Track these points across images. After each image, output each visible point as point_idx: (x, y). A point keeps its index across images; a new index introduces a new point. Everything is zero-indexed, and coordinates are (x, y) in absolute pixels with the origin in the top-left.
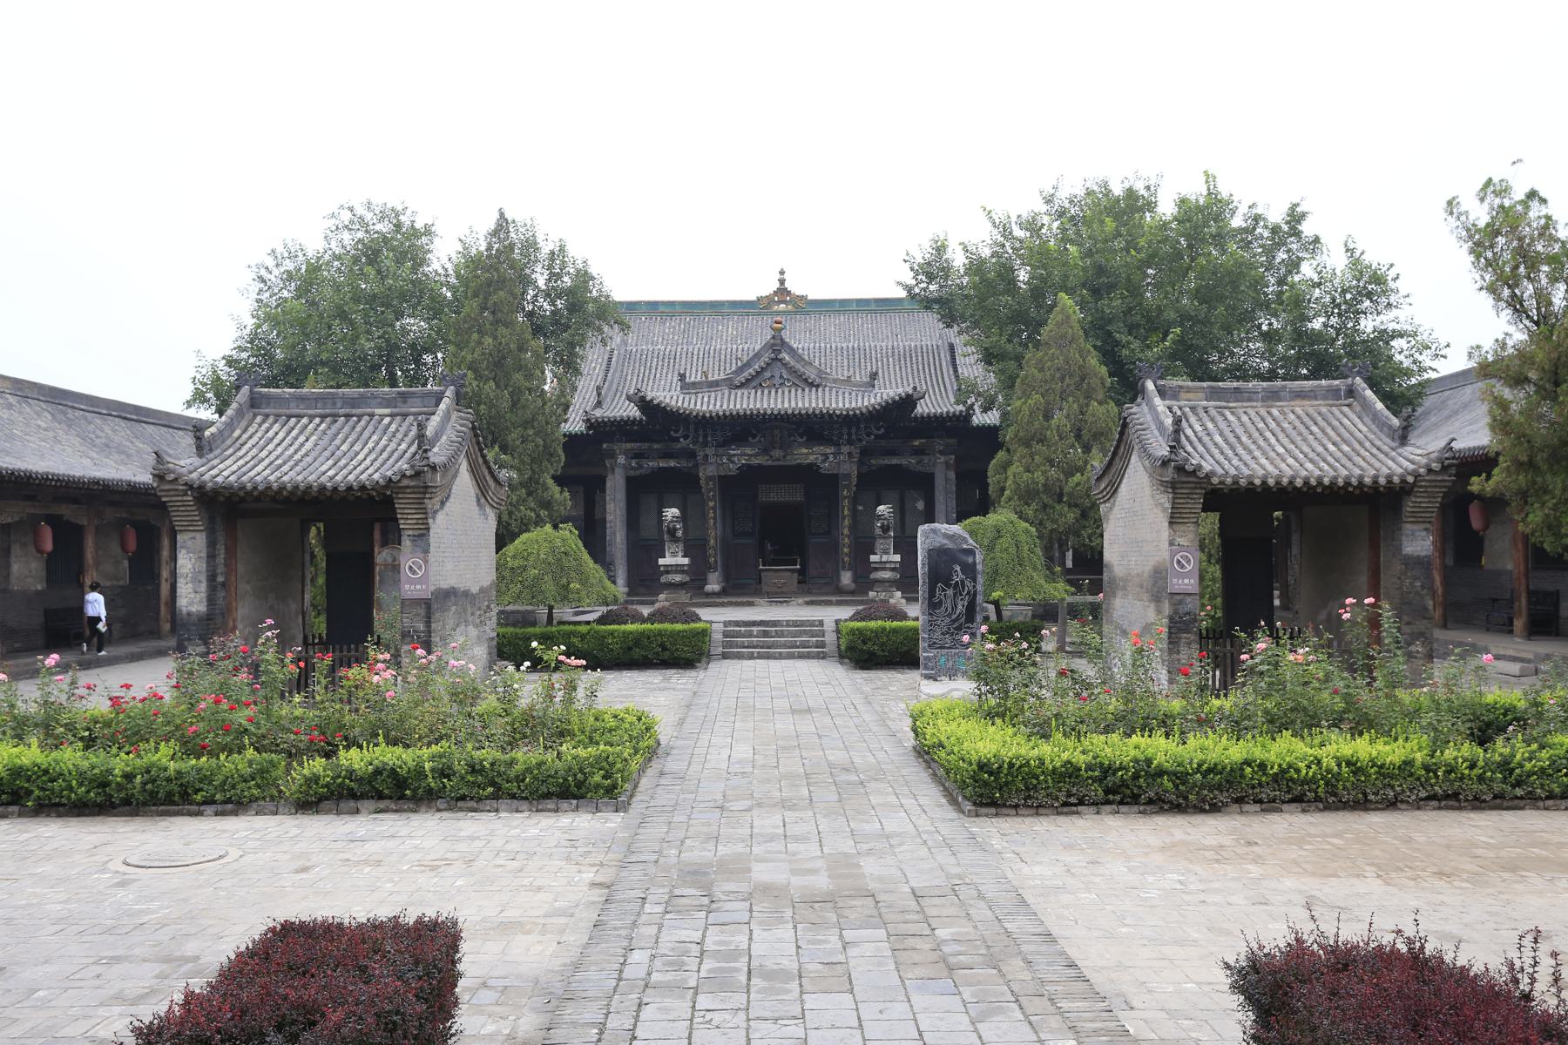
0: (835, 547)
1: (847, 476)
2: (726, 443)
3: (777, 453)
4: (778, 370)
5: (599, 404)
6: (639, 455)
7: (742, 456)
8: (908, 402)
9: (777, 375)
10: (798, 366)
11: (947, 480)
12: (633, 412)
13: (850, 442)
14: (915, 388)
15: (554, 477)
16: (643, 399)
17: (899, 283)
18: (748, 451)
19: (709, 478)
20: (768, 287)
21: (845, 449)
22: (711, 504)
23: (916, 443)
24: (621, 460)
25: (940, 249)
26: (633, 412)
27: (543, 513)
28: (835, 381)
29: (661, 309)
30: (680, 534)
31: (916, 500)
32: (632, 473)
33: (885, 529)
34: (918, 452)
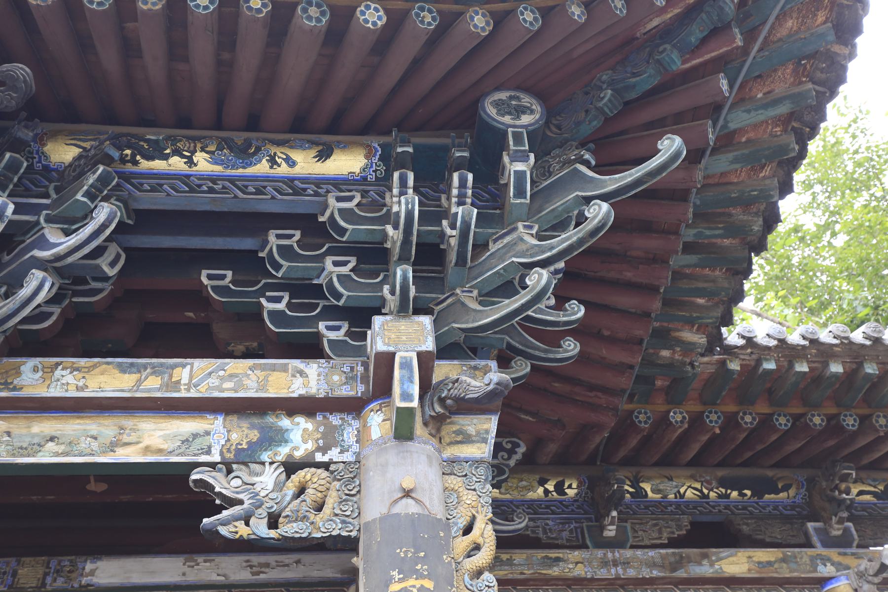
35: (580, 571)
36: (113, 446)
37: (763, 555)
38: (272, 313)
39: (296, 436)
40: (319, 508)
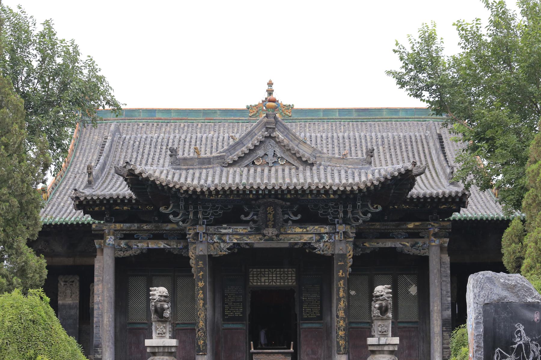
0: (326, 333)
1: (343, 257)
2: (218, 222)
3: (270, 232)
4: (271, 148)
5: (90, 183)
6: (128, 236)
7: (234, 236)
8: (406, 179)
9: (271, 154)
10: (292, 145)
11: (441, 263)
12: (121, 189)
13: (346, 222)
14: (414, 164)
15: (30, 243)
16: (131, 173)
17: (389, 73)
18: (240, 229)
19: (199, 258)
20: (256, 97)
21: (341, 228)
22: (201, 284)
23: (411, 226)
24: (110, 240)
25: (429, 39)
26: (121, 189)
27: (16, 280)
28: (330, 159)
29: (158, 116)
30: (167, 314)
31: (408, 285)
32: (121, 254)
33: (383, 310)
34: (413, 235)
35: (378, 227)
36: (300, 239)
37: (417, 224)
38: (321, 213)
39: (325, 238)
40: (329, 249)
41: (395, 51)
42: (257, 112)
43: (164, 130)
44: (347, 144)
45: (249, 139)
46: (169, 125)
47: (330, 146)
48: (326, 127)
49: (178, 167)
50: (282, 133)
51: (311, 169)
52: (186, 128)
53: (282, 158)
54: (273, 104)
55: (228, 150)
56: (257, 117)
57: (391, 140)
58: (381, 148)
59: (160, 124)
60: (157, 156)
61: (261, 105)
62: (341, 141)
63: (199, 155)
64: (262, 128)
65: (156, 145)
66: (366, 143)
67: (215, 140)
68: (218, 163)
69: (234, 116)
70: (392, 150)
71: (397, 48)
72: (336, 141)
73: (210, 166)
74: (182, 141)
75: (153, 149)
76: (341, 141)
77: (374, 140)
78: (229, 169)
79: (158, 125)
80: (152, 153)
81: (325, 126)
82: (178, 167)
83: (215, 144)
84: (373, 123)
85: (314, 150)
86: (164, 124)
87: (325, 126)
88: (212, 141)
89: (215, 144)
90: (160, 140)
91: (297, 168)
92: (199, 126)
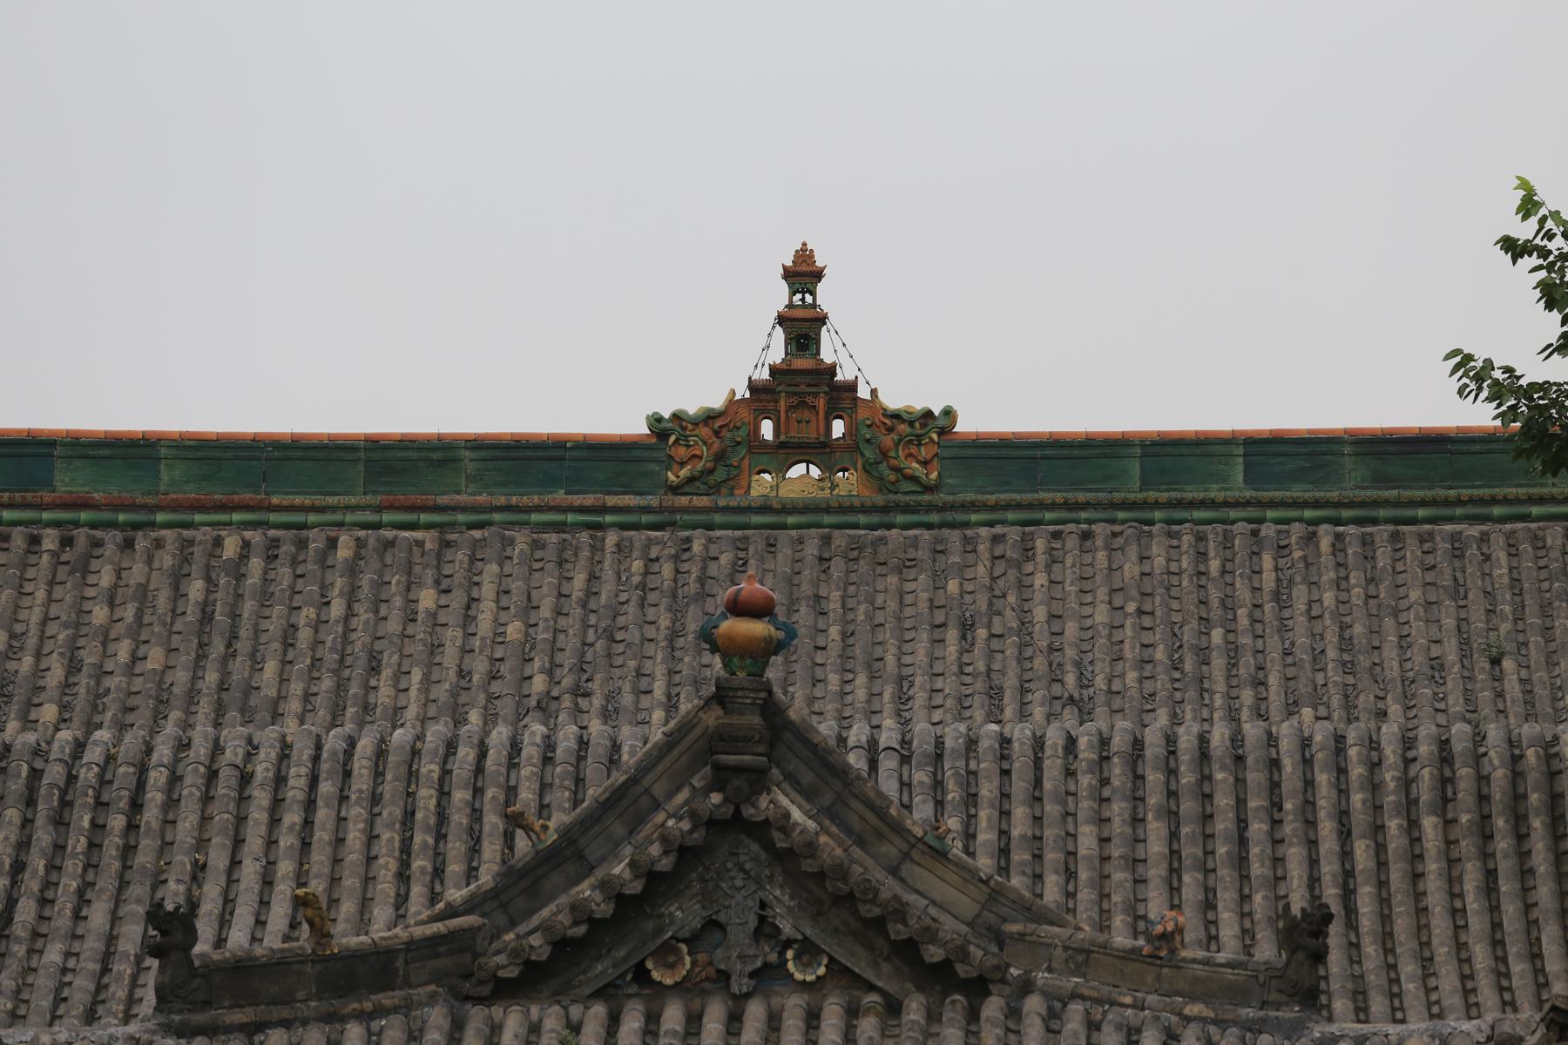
9: (740, 918)
10: (867, 868)
20: (715, 360)
28: (1082, 957)
29: (68, 481)
41: (1514, 248)
42: (720, 457)
43: (106, 579)
44: (1223, 800)
45: (619, 829)
46: (141, 543)
47: (1118, 810)
48: (1160, 562)
49: (199, 1018)
50: (808, 794)
51: (973, 1015)
52: (256, 564)
53: (808, 950)
54: (757, 628)
55: (494, 894)
56: (714, 489)
57: (1500, 775)
58: (1429, 824)
59: (81, 536)
60: (68, 883)
61: (745, 415)
62: (1187, 778)
63: (321, 934)
64: (692, 769)
65: (66, 804)
66: (1343, 792)
67: (429, 768)
68: (436, 978)
69: (575, 483)
70: (1502, 844)
71: (1525, 231)
72: (1154, 778)
73: (387, 999)
74: (227, 777)
75: (43, 836)
76: (1187, 778)
77: (1389, 777)
78: (497, 1011)
79: (67, 542)
80: (38, 864)
81: (1158, 550)
82: (199, 1018)
83: (426, 797)
84: (1474, 531)
85: (995, 895)
86: (111, 538)
87: (1158, 550)
88: (412, 775)
89: (426, 797)
90: (87, 775)
91: (893, 1008)
92: (344, 552)
